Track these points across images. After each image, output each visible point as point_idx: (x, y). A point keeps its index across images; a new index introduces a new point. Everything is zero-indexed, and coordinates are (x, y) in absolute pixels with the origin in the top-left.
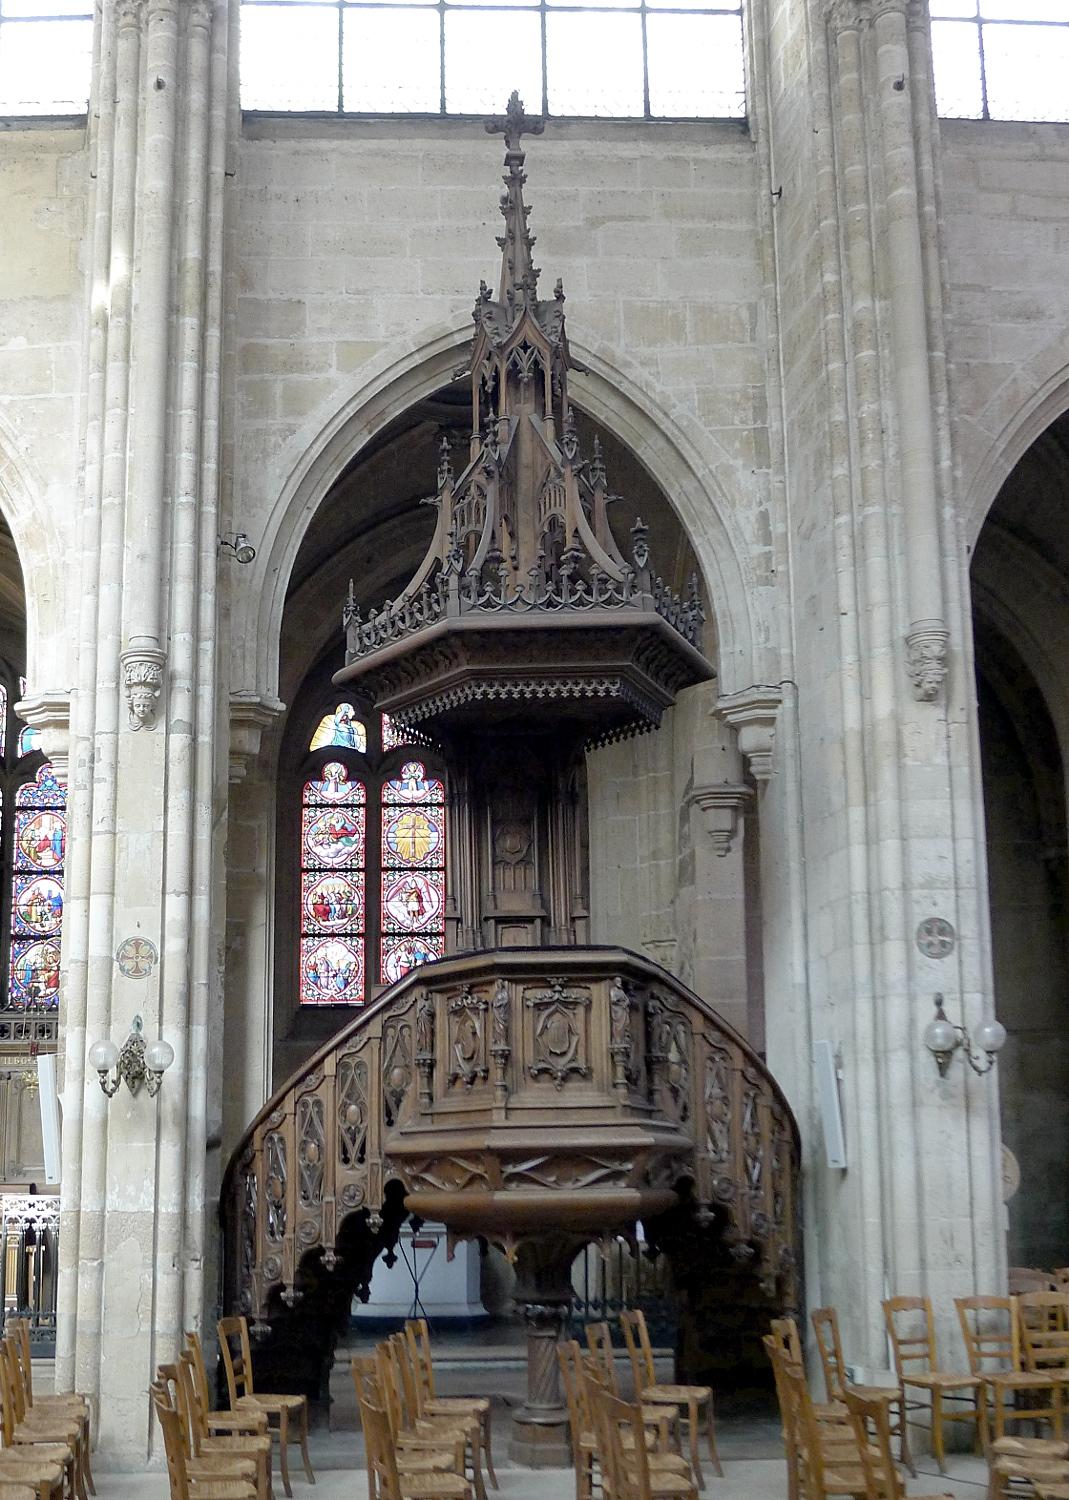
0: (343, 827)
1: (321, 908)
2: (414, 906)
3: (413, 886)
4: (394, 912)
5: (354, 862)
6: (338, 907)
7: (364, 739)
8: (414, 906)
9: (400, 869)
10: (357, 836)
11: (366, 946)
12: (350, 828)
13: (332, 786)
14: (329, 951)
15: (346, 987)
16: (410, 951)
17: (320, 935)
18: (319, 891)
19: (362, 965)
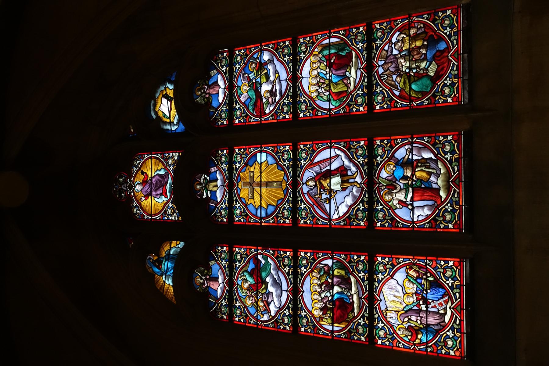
0: (251, 274)
1: (338, 313)
2: (335, 182)
3: (312, 183)
4: (343, 209)
5: (286, 262)
6: (336, 289)
7: (174, 244)
8: (335, 182)
9: (295, 202)
10: (260, 257)
11: (385, 252)
12: (251, 266)
13: (213, 285)
14: (391, 306)
15: (442, 286)
16: (391, 186)
17: (371, 318)
18: (317, 313)
19: (410, 259)
